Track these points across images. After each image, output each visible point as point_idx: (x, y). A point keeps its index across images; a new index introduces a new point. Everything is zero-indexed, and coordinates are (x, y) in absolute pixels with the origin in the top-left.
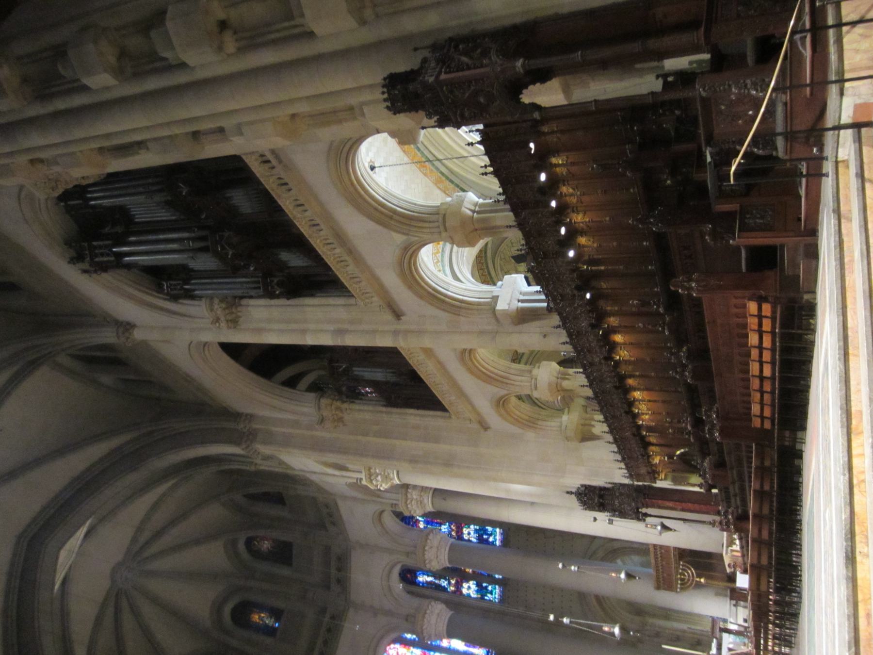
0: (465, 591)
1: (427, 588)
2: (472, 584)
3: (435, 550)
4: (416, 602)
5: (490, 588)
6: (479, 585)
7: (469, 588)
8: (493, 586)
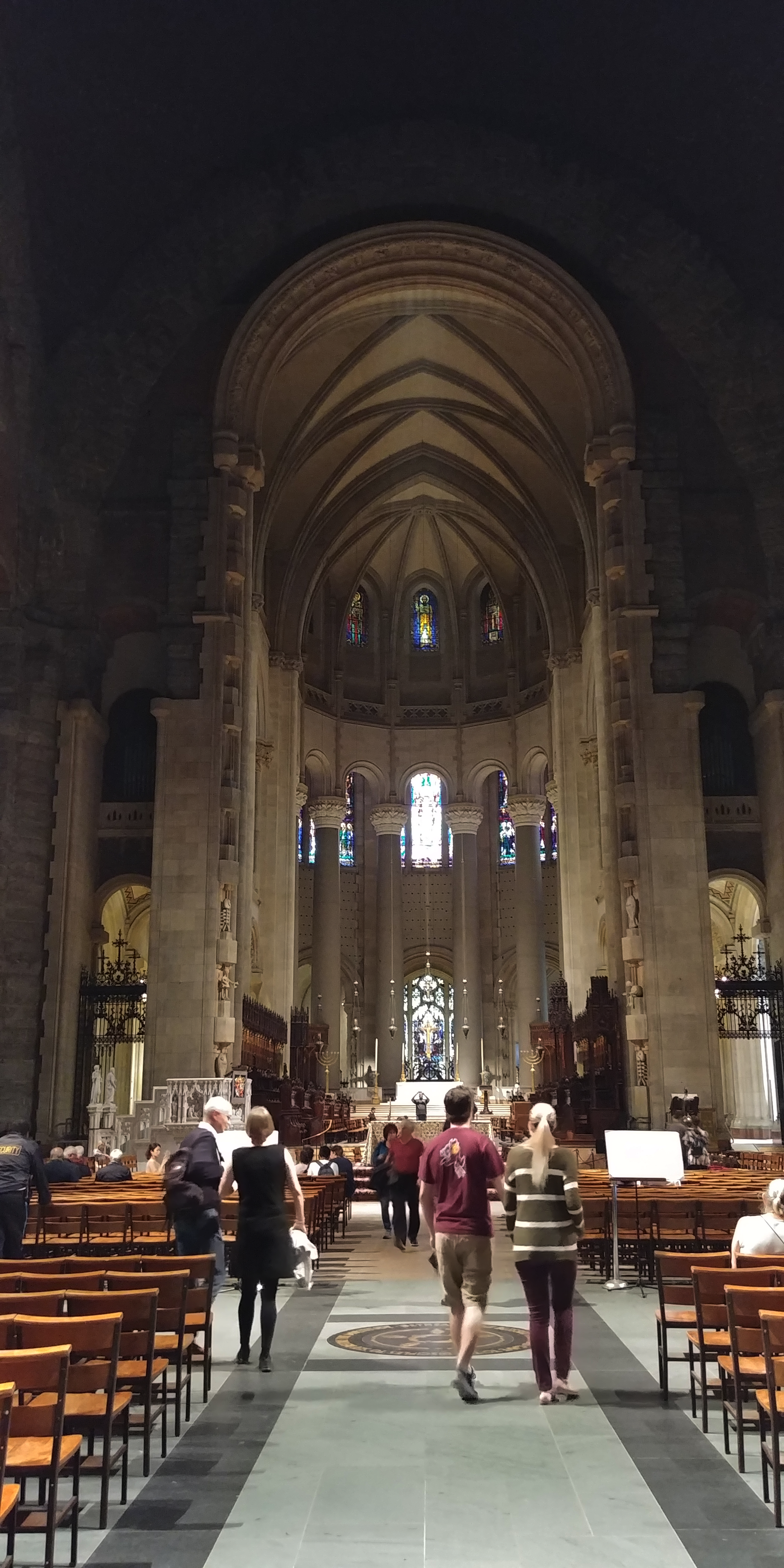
0: (504, 825)
1: (499, 783)
2: (511, 832)
3: (525, 812)
4: (477, 796)
5: (512, 851)
6: (512, 837)
7: (507, 829)
8: (514, 854)
